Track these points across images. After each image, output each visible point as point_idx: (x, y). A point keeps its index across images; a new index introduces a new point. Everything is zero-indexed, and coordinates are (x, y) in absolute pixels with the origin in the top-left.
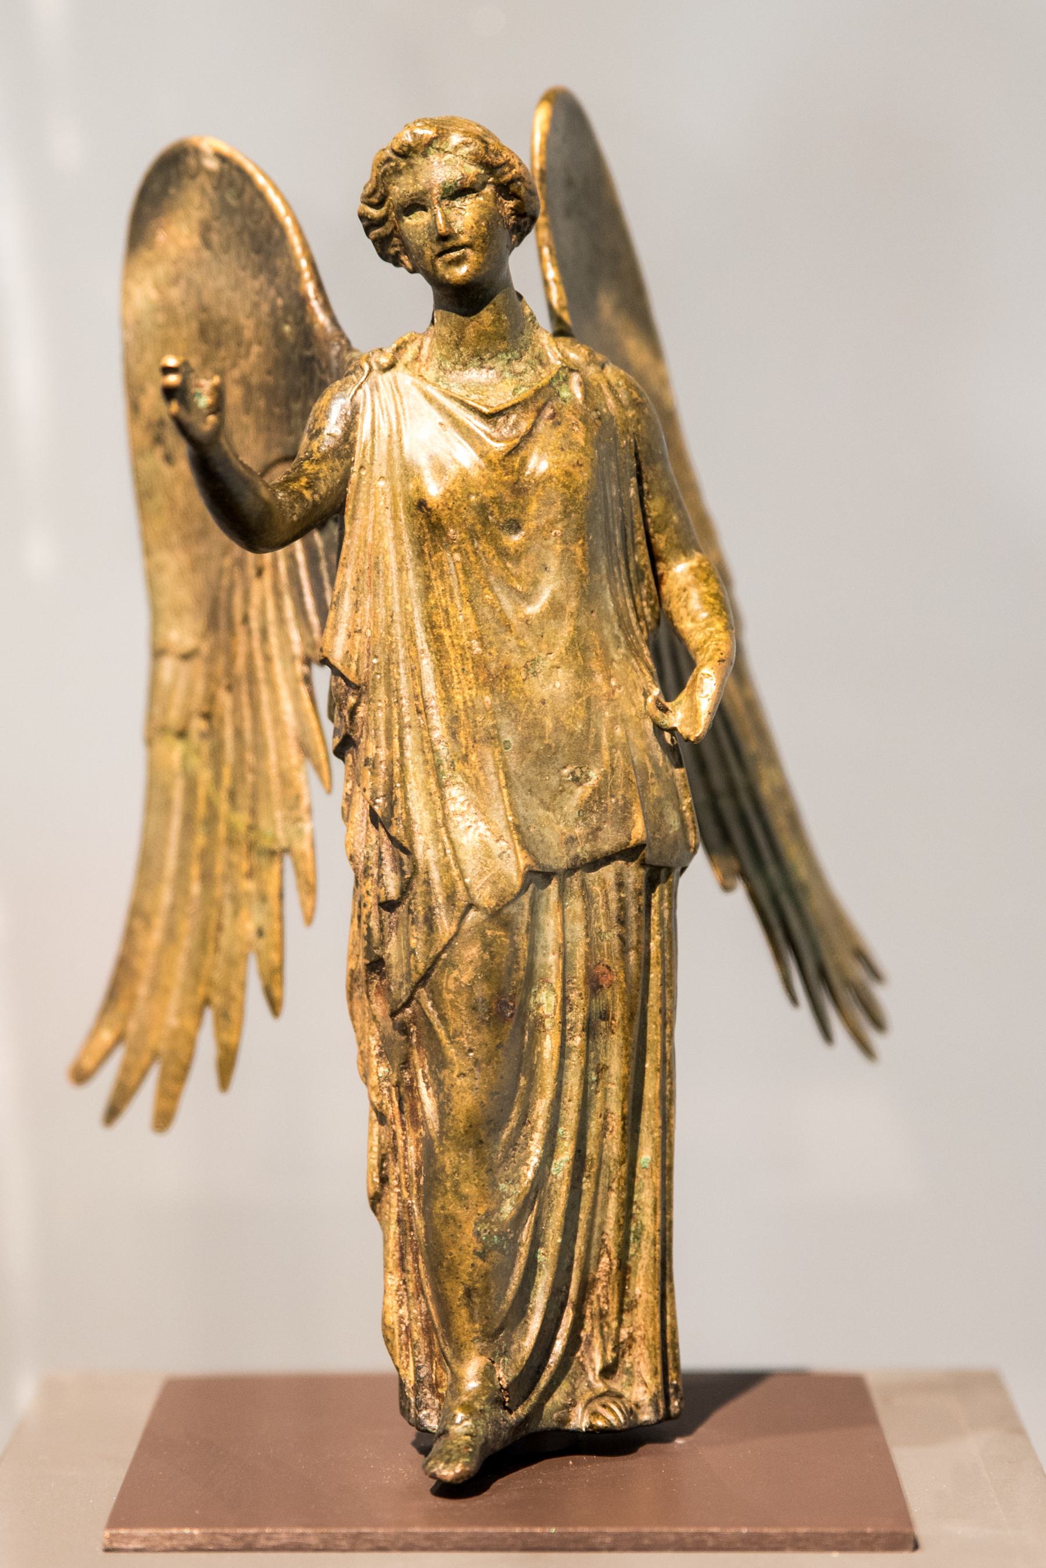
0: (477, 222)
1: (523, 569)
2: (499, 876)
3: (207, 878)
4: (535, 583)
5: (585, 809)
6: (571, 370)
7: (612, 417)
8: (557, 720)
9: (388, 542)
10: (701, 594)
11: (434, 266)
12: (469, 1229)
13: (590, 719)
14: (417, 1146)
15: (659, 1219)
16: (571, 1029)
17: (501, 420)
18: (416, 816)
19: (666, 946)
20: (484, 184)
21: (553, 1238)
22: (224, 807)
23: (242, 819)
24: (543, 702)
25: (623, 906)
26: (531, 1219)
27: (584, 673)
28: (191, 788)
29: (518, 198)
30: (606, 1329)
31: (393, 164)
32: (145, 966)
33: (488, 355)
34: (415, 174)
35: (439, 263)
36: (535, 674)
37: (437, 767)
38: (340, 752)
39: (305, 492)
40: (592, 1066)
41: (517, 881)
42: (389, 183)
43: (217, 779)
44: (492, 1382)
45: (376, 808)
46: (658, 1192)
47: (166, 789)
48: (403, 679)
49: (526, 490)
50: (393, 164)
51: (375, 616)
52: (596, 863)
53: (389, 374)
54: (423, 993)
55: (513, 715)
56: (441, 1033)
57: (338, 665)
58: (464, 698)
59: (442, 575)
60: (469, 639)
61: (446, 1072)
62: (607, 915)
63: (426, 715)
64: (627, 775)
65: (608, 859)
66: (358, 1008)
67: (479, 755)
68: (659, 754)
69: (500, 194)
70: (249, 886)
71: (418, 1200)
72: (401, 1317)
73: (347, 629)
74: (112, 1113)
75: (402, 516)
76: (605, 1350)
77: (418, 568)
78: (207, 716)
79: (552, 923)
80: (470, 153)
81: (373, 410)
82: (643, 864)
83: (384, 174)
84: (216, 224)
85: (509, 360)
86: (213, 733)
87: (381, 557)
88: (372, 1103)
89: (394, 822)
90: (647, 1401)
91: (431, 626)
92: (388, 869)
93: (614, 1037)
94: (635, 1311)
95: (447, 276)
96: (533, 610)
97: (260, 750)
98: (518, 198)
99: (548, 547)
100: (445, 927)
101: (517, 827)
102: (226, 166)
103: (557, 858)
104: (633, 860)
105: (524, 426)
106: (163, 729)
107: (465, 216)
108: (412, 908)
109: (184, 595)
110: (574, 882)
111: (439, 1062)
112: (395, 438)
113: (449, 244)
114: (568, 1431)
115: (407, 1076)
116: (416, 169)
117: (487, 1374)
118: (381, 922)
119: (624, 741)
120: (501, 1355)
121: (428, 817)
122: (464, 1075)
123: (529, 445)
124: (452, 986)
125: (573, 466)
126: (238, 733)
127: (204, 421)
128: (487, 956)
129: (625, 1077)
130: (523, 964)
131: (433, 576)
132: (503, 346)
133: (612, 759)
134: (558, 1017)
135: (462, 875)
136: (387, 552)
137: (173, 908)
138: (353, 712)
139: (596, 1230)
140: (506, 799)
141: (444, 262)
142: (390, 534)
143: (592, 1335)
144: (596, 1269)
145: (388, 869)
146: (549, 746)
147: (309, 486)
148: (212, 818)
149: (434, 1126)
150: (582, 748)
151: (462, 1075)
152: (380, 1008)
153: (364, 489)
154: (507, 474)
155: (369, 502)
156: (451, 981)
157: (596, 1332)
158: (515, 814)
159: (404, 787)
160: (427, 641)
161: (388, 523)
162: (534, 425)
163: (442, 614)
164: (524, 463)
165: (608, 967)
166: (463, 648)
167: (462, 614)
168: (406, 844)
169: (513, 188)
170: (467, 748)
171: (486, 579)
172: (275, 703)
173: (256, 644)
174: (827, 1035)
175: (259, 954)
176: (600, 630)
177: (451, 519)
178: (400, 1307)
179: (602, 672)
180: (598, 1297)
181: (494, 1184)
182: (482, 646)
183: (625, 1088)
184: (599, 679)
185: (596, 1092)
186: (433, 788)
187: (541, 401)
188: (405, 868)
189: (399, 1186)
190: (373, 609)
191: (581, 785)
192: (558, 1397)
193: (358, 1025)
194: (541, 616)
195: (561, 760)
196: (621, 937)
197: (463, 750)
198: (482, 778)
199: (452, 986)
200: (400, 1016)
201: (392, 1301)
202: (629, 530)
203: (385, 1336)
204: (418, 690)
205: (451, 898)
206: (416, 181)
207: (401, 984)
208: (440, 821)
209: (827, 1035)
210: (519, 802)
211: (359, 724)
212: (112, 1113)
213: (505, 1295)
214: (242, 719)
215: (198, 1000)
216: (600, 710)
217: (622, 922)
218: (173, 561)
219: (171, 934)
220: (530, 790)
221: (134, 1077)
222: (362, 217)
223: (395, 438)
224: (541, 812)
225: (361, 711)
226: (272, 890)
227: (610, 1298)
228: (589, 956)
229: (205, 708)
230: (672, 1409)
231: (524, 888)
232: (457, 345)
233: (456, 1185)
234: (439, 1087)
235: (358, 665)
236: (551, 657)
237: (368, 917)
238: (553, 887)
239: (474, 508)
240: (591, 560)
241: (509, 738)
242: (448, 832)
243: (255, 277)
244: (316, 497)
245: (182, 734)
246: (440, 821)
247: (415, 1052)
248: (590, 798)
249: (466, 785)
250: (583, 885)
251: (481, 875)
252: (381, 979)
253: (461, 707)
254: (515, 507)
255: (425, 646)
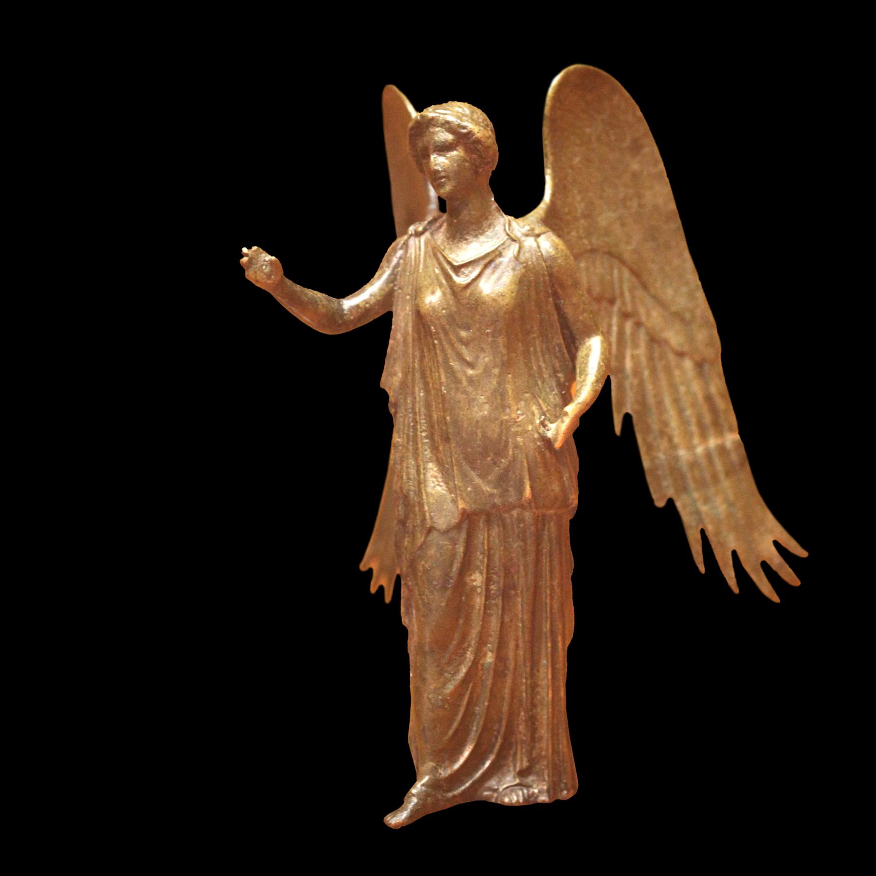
100: (420, 539)
124: (421, 569)
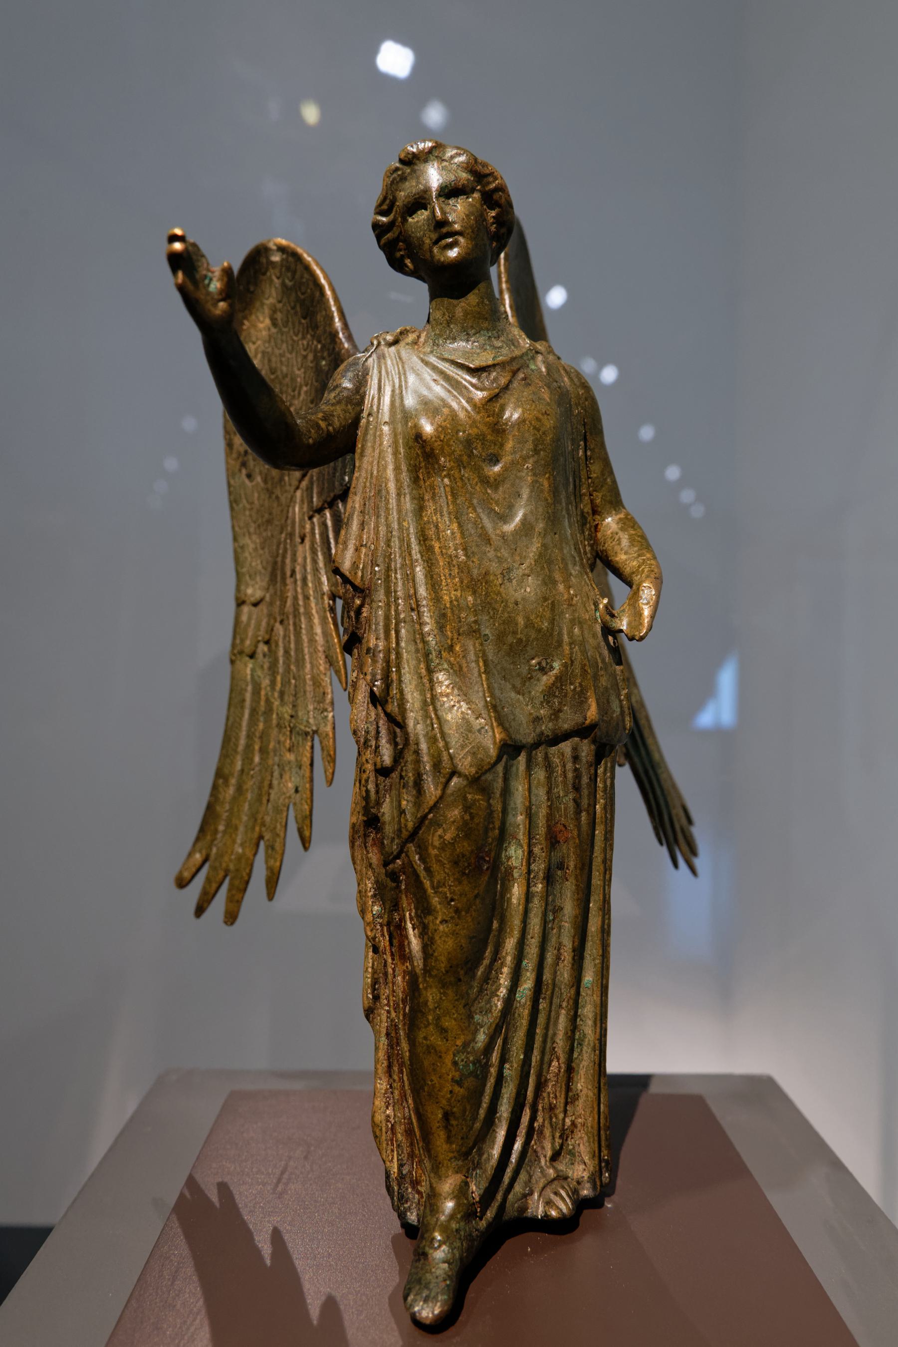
0: (467, 216)
1: (499, 495)
2: (478, 748)
3: (263, 751)
4: (511, 507)
5: (549, 693)
6: (537, 352)
7: (568, 391)
8: (527, 618)
9: (390, 473)
10: (630, 536)
11: (431, 251)
12: (448, 1059)
13: (554, 619)
14: (404, 978)
15: (598, 1030)
16: (534, 878)
17: (484, 375)
18: (409, 697)
19: (608, 808)
20: (473, 190)
21: (517, 1054)
22: (277, 703)
23: (287, 710)
24: (516, 603)
25: (578, 776)
26: (500, 1041)
27: (549, 582)
28: (257, 691)
29: (500, 206)
30: (554, 1120)
31: (399, 173)
32: (223, 810)
33: (473, 331)
34: (418, 178)
35: (435, 250)
36: (510, 580)
37: (427, 655)
38: (348, 648)
39: (320, 422)
40: (550, 908)
41: (493, 752)
42: (396, 190)
43: (273, 683)
44: (467, 1199)
45: (375, 689)
46: (598, 1008)
47: (243, 691)
48: (400, 584)
49: (504, 431)
50: (399, 173)
51: (377, 533)
52: (557, 739)
53: (393, 349)
54: (411, 847)
55: (492, 613)
56: (427, 884)
57: (347, 573)
58: (450, 598)
59: (433, 497)
60: (456, 550)
61: (431, 918)
62: (565, 783)
63: (418, 612)
64: (583, 667)
65: (566, 736)
66: (358, 855)
67: (463, 646)
68: (606, 652)
69: (485, 204)
70: (291, 757)
71: (404, 1025)
72: (388, 1116)
73: (355, 544)
74: (200, 911)
75: (402, 451)
76: (554, 1138)
77: (414, 492)
78: (267, 642)
79: (520, 788)
80: (462, 162)
81: (380, 372)
82: (594, 742)
83: (392, 182)
84: (279, 306)
85: (490, 337)
86: (272, 654)
87: (384, 485)
88: (367, 936)
89: (390, 700)
90: (586, 1178)
91: (423, 539)
92: (383, 741)
93: (568, 883)
94: (577, 1103)
95: (442, 259)
96: (509, 527)
97: (300, 662)
98: (500, 206)
99: (521, 478)
100: (432, 790)
101: (494, 707)
102: (284, 256)
103: (527, 735)
104: (586, 738)
105: (503, 381)
106: (241, 653)
107: (458, 211)
108: (404, 774)
109: (257, 564)
110: (539, 755)
111: (424, 910)
112: (397, 391)
113: (444, 230)
114: (527, 1218)
115: (396, 917)
116: (418, 173)
117: (461, 1192)
118: (377, 785)
119: (581, 638)
120: (474, 1170)
121: (418, 697)
122: (446, 921)
123: (506, 396)
124: (437, 843)
125: (542, 414)
126: (287, 652)
127: (215, 305)
128: (467, 817)
129: (576, 917)
130: (497, 824)
131: (426, 498)
132: (486, 325)
133: (572, 653)
134: (524, 869)
135: (447, 747)
136: (388, 480)
137: (242, 771)
138: (358, 612)
139: (549, 1040)
140: (485, 683)
141: (440, 247)
142: (391, 467)
143: (543, 1126)
144: (548, 1072)
145: (383, 741)
146: (520, 640)
147: (324, 419)
148: (269, 710)
149: (419, 963)
150: (548, 643)
151: (444, 921)
152: (375, 857)
153: (371, 432)
154: (488, 416)
155: (375, 442)
156: (436, 838)
157: (547, 1123)
158: (492, 695)
159: (399, 671)
160: (420, 552)
161: (389, 458)
162: (510, 382)
163: (433, 529)
164: (502, 410)
165: (564, 826)
166: (450, 556)
167: (450, 529)
168: (399, 719)
169: (496, 196)
170: (452, 639)
171: (471, 501)
172: (311, 627)
173: (299, 590)
174: (676, 865)
175: (295, 804)
176: (561, 549)
177: (442, 449)
178: (387, 1108)
179: (563, 582)
180: (549, 1093)
181: (470, 1017)
182: (466, 555)
183: (575, 925)
184: (561, 587)
185: (553, 929)
186: (423, 672)
187: (515, 366)
188: (398, 740)
189: (388, 1005)
190: (377, 527)
191: (546, 673)
192: (518, 1188)
193: (359, 868)
194: (516, 532)
195: (530, 651)
196: (574, 800)
197: (449, 641)
198: (465, 665)
199: (437, 843)
200: (391, 866)
201: (379, 1102)
202: (577, 484)
203: (374, 1133)
204: (412, 591)
205: (437, 766)
206: (418, 183)
207: (393, 839)
208: (429, 700)
209: (676, 865)
210: (496, 685)
211: (364, 623)
212: (200, 911)
213: (478, 1114)
214: (289, 642)
215: (256, 835)
216: (562, 612)
217: (577, 788)
218: (250, 543)
219: (240, 789)
220: (504, 677)
221: (214, 886)
222: (376, 226)
223: (397, 391)
224: (513, 695)
225: (365, 612)
226: (306, 760)
227: (558, 1095)
228: (550, 817)
229: (267, 637)
230: (603, 1179)
231: (499, 759)
232: (448, 324)
233: (438, 1019)
234: (424, 931)
235: (362, 572)
236: (523, 567)
237: (367, 781)
238: (522, 759)
239: (461, 442)
240: (555, 492)
241: (487, 632)
242: (435, 710)
243: (303, 338)
244: (331, 428)
245: (252, 656)
246: (429, 700)
247: (404, 897)
248: (553, 684)
249: (451, 671)
250: (546, 757)
251: (463, 747)
252: (377, 833)
253: (448, 605)
254: (495, 444)
255: (419, 556)
